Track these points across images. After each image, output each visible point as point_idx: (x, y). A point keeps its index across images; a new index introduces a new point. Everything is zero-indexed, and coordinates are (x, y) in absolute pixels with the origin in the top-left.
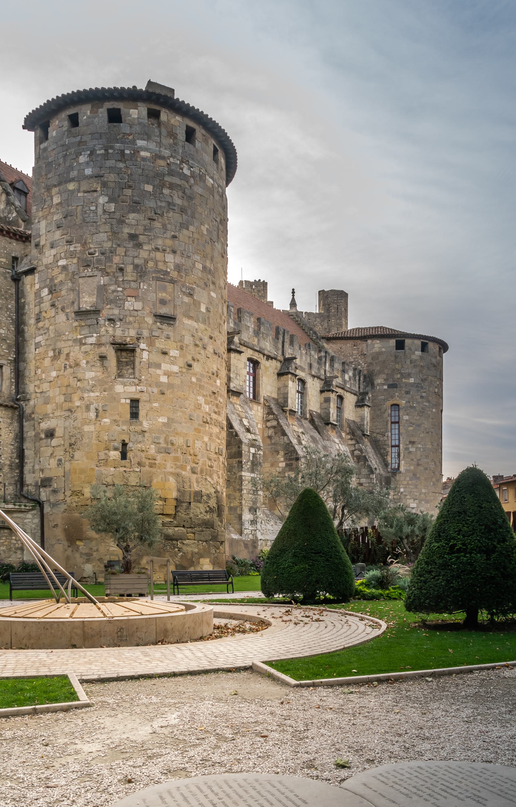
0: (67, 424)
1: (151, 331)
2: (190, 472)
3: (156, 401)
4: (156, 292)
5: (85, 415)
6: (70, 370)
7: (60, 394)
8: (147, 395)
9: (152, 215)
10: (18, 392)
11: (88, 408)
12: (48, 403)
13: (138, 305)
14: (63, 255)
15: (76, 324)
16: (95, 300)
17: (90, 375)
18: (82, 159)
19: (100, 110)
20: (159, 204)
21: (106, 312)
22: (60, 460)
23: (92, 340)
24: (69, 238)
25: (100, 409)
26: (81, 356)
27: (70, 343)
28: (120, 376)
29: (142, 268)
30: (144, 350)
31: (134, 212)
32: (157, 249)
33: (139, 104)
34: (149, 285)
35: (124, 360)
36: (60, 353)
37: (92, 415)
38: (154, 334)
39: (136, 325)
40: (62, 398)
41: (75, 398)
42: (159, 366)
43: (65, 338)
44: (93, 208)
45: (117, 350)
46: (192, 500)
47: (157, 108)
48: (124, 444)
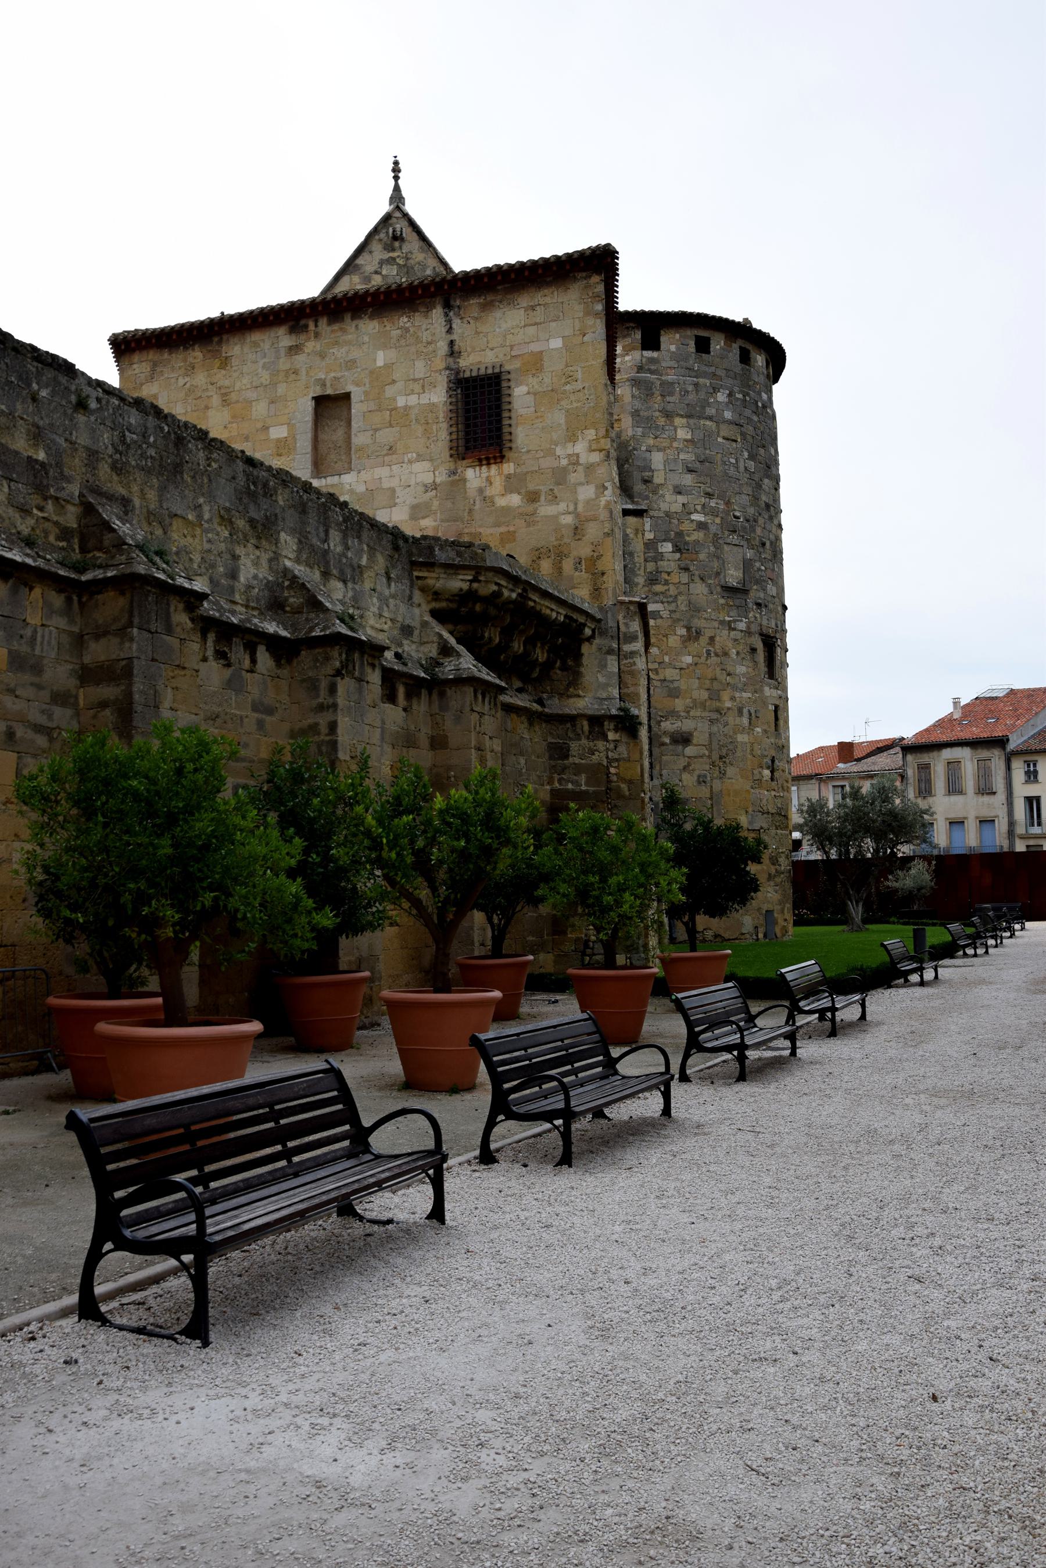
0: (715, 729)
5: (738, 720)
6: (714, 660)
7: (700, 688)
12: (678, 697)
14: (699, 508)
15: (722, 601)
16: (741, 575)
17: (741, 669)
18: (722, 397)
19: (734, 345)
21: (755, 593)
22: (705, 776)
23: (742, 626)
24: (709, 490)
36: (699, 633)
37: (745, 721)
40: (705, 695)
41: (725, 696)
43: (705, 616)
44: (733, 461)
48: (773, 761)
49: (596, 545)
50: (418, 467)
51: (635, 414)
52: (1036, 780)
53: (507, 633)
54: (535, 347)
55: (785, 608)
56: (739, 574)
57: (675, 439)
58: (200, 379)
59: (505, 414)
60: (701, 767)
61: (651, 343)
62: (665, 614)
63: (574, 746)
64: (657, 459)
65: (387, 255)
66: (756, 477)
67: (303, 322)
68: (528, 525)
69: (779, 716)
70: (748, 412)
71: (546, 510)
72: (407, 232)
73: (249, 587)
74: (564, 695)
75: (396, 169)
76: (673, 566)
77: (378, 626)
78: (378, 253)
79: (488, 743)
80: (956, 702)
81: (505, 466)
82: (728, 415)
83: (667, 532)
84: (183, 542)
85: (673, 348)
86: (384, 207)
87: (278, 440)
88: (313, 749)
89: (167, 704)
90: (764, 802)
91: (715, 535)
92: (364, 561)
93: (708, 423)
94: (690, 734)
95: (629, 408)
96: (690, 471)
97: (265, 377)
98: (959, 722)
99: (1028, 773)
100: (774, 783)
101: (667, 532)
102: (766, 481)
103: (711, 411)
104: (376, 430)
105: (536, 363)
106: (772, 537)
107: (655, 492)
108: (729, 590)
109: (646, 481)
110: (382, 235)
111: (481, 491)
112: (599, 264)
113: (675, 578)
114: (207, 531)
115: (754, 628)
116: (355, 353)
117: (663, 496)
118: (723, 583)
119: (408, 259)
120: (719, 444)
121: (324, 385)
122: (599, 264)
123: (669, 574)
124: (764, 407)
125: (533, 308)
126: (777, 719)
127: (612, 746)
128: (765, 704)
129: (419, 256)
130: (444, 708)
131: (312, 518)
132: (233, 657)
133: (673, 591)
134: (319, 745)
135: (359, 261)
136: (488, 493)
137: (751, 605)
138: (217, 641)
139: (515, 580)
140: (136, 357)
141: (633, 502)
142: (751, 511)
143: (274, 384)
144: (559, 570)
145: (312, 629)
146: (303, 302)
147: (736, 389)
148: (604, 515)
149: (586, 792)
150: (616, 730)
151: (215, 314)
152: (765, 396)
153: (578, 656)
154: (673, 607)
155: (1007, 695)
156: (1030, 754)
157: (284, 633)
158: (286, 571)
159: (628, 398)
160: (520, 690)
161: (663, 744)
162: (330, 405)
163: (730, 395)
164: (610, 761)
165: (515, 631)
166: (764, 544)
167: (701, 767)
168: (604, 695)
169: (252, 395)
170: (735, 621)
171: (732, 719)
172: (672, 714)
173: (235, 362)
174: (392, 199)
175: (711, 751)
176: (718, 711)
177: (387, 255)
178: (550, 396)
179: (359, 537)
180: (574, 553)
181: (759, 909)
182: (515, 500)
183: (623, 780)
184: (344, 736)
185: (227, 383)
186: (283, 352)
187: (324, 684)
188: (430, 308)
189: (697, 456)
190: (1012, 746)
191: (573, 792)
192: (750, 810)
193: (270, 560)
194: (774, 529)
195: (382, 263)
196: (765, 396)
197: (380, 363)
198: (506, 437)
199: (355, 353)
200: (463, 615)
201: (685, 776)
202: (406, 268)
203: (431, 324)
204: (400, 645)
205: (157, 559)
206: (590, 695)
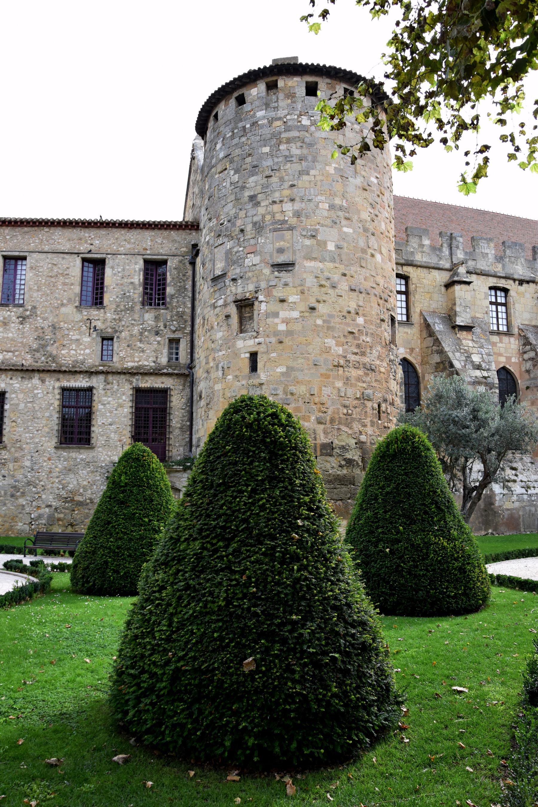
1: (268, 281)
2: (316, 422)
3: (274, 351)
4: (273, 243)
8: (264, 346)
9: (267, 173)
13: (256, 259)
19: (231, 101)
20: (276, 160)
23: (221, 302)
25: (225, 367)
28: (241, 331)
29: (260, 224)
30: (262, 301)
31: (253, 176)
32: (274, 202)
33: (258, 82)
34: (267, 238)
35: (248, 315)
37: (220, 373)
38: (271, 284)
39: (255, 279)
42: (276, 315)
46: (319, 453)
47: (274, 78)
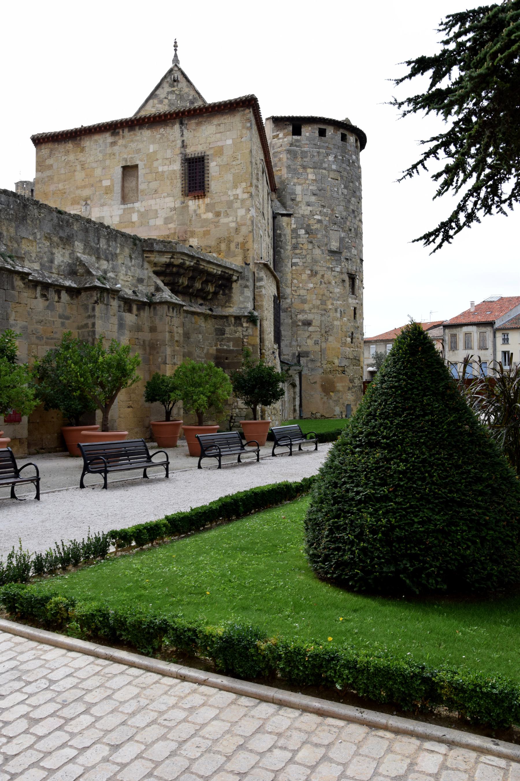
0: (323, 319)
5: (335, 314)
6: (324, 285)
7: (316, 299)
10: (278, 293)
11: (336, 310)
14: (318, 213)
15: (328, 258)
17: (337, 290)
18: (331, 158)
21: (345, 254)
23: (338, 269)
24: (323, 204)
26: (332, 278)
27: (325, 269)
36: (316, 273)
37: (338, 315)
40: (319, 302)
41: (329, 303)
44: (336, 189)
45: (349, 277)
48: (352, 334)
49: (245, 237)
50: (168, 200)
51: (288, 167)
52: (508, 343)
53: (192, 279)
54: (220, 144)
55: (362, 260)
56: (337, 244)
57: (307, 179)
58: (71, 157)
59: (206, 175)
60: (316, 337)
61: (297, 132)
62: (301, 264)
63: (227, 329)
64: (298, 189)
65: (171, 89)
66: (348, 197)
67: (117, 131)
68: (216, 227)
69: (357, 313)
70: (344, 165)
71: (223, 220)
72: (180, 78)
73: (60, 266)
74: (224, 306)
75: (176, 46)
76: (304, 241)
77: (125, 279)
78: (166, 88)
79: (175, 329)
80: (472, 303)
81: (206, 199)
82: (334, 167)
83: (302, 225)
84: (27, 249)
85: (307, 134)
86: (170, 65)
87: (106, 187)
88: (86, 334)
89: (12, 318)
90: (347, 353)
91: (326, 226)
92: (118, 251)
93: (324, 171)
94: (311, 321)
95: (285, 164)
96: (314, 195)
97: (100, 156)
98: (473, 313)
99: (504, 339)
100: (352, 345)
101: (302, 225)
102: (353, 199)
103: (325, 165)
104: (149, 182)
105: (220, 151)
106: (355, 226)
107: (297, 205)
108: (332, 252)
109: (293, 200)
110: (168, 79)
111: (195, 211)
112: (250, 103)
113: (305, 247)
114: (39, 243)
115: (344, 270)
116: (141, 146)
117: (301, 207)
118: (329, 249)
119: (181, 91)
120: (329, 181)
121: (126, 161)
122: (250, 103)
123: (303, 244)
124: (353, 162)
125: (219, 125)
126: (355, 313)
127: (245, 329)
128: (349, 307)
129: (186, 90)
130: (155, 314)
131: (91, 235)
132: (49, 297)
133: (304, 253)
134: (88, 332)
135: (158, 92)
136: (198, 212)
137: (343, 259)
138: (42, 290)
139: (192, 257)
140: (43, 146)
141: (286, 210)
142: (344, 214)
143: (104, 160)
144: (229, 248)
145: (86, 284)
146: (117, 121)
147: (339, 154)
148: (249, 223)
149: (233, 350)
150: (247, 322)
151: (78, 126)
152: (354, 157)
153: (231, 288)
154: (304, 260)
155: (499, 300)
156: (505, 330)
157: (74, 285)
158: (78, 258)
159: (285, 160)
160: (201, 305)
161: (298, 326)
162: (129, 170)
163: (335, 157)
164: (244, 336)
165: (195, 280)
166: (350, 230)
167: (316, 337)
168: (243, 306)
169: (94, 165)
170: (334, 267)
171: (332, 314)
172: (303, 311)
173: (87, 149)
174: (173, 61)
175: (321, 329)
176: (325, 310)
177: (171, 89)
178: (225, 167)
179: (116, 241)
180: (236, 240)
181: (343, 404)
182: (210, 215)
183: (250, 345)
184: (99, 329)
185: (83, 159)
186: (108, 145)
187: (90, 307)
188: (173, 124)
189: (318, 187)
190: (496, 326)
191: (226, 350)
192: (340, 357)
193: (70, 254)
194: (357, 222)
195: (168, 93)
196: (354, 157)
197: (151, 151)
198: (206, 186)
199: (141, 146)
200: (169, 274)
201: (309, 341)
202: (180, 97)
203: (174, 132)
204: (137, 287)
205: (9, 260)
206: (236, 306)
